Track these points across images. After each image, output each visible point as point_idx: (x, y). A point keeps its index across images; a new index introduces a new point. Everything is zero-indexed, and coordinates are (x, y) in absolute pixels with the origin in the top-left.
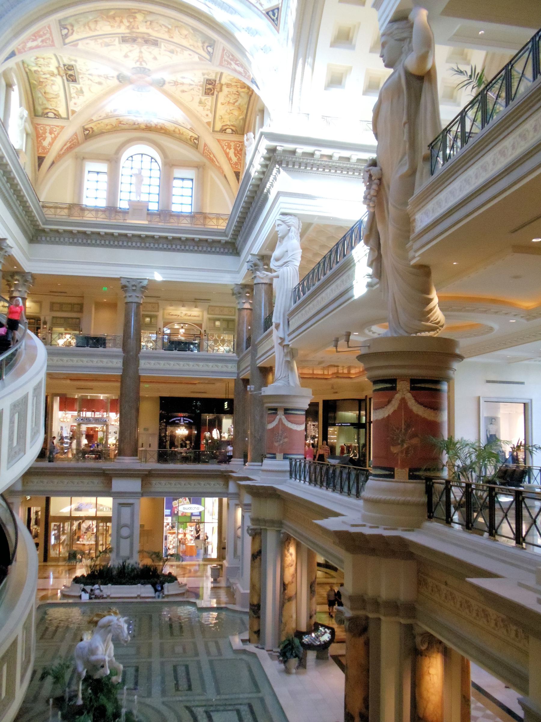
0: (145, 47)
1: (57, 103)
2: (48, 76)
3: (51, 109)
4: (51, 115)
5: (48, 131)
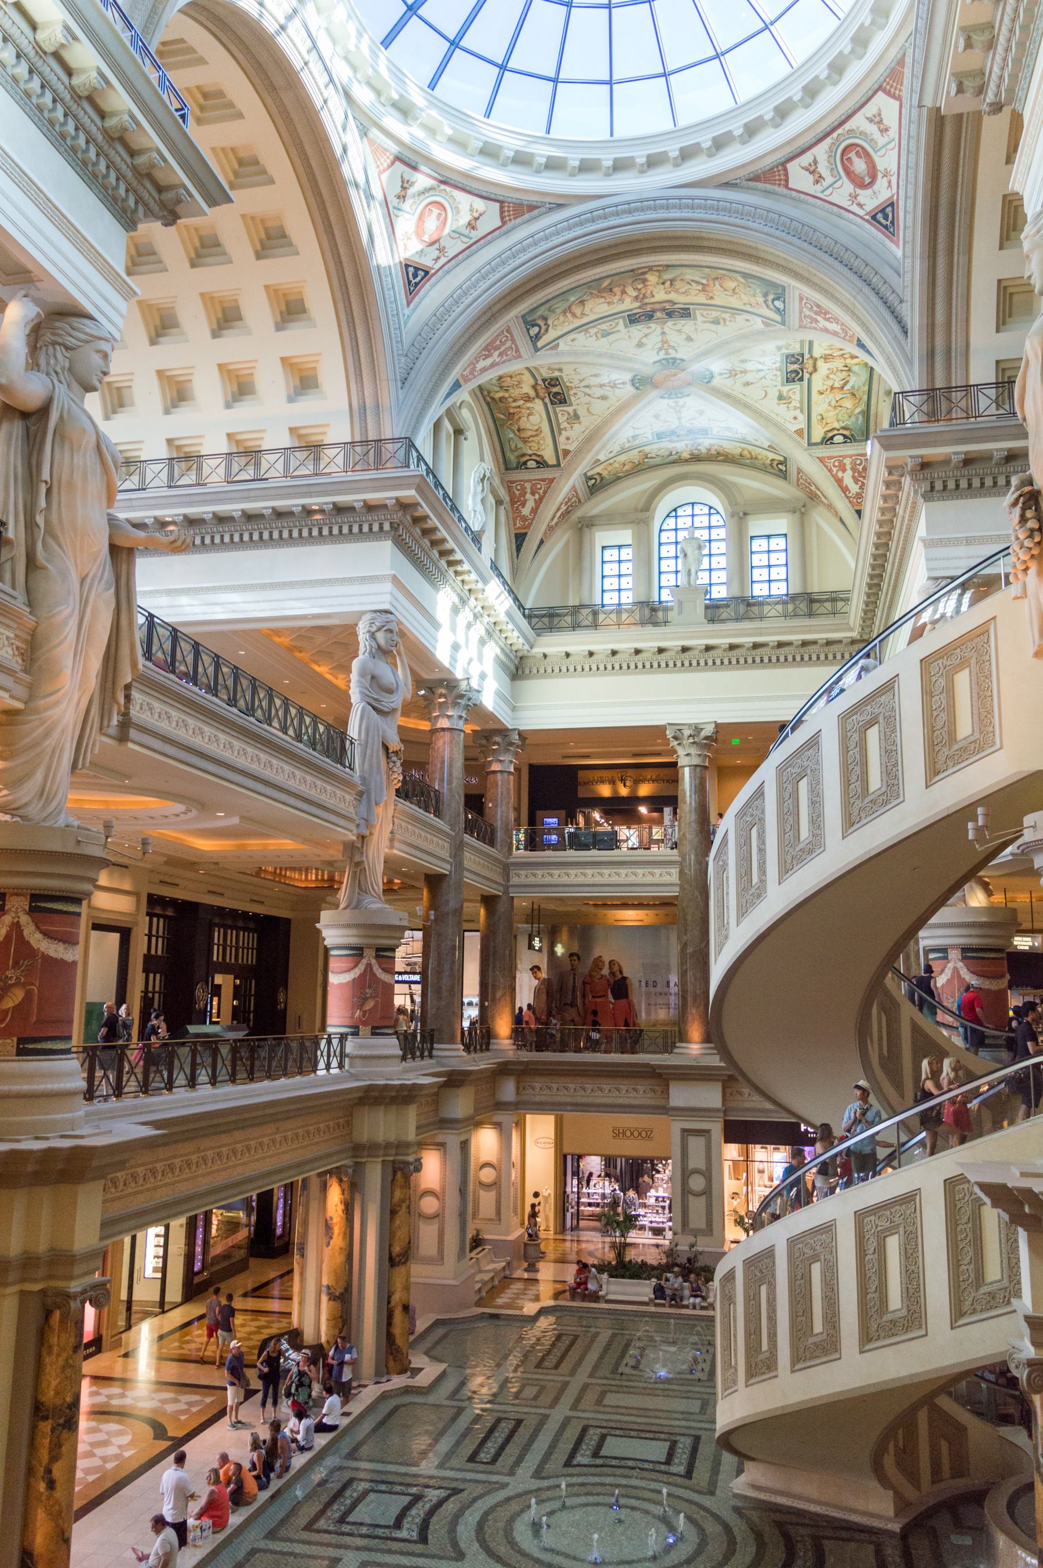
0: (670, 323)
2: (521, 403)
4: (531, 464)
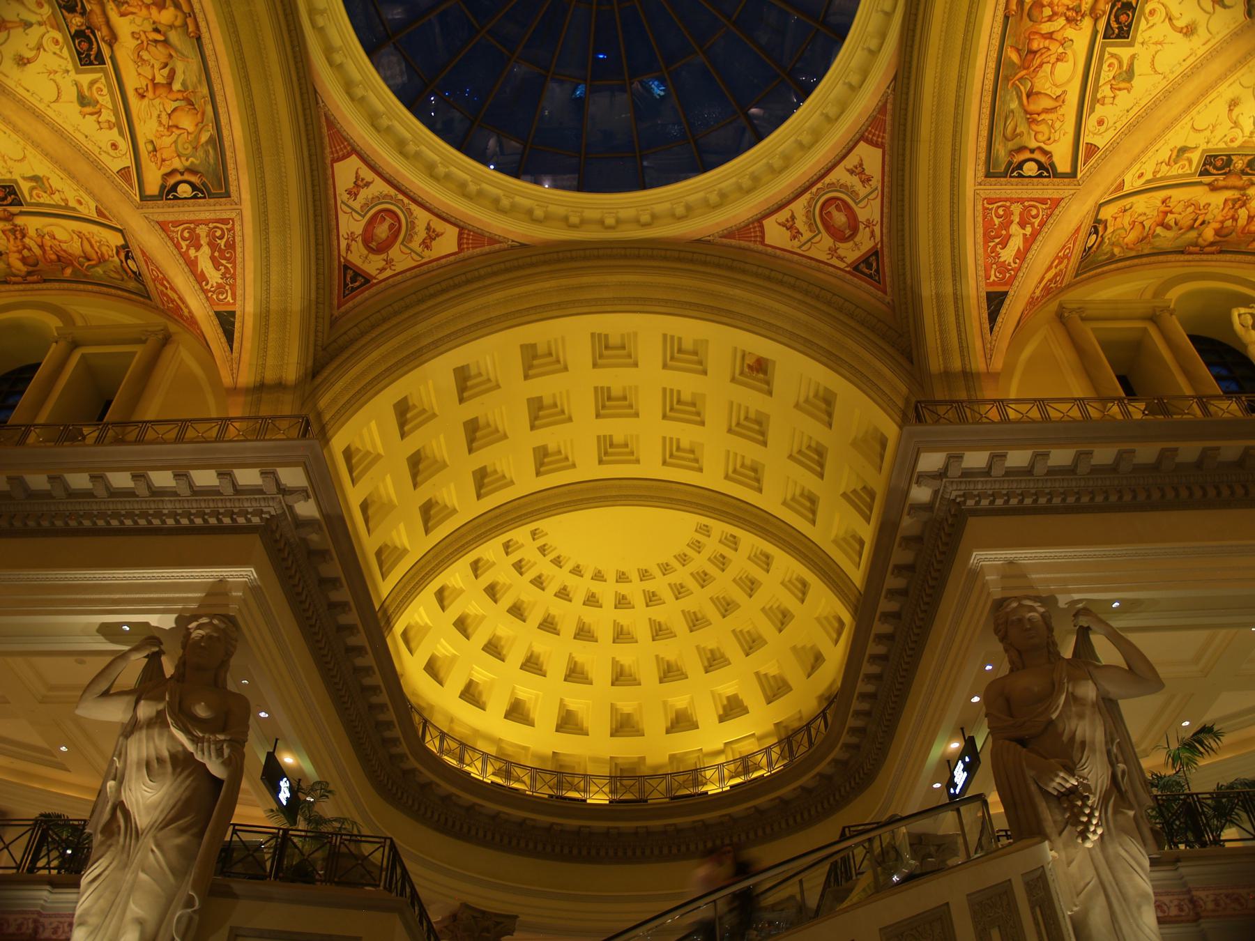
1: (1052, 126)
3: (1032, 151)
4: (1030, 169)
5: (1016, 219)
